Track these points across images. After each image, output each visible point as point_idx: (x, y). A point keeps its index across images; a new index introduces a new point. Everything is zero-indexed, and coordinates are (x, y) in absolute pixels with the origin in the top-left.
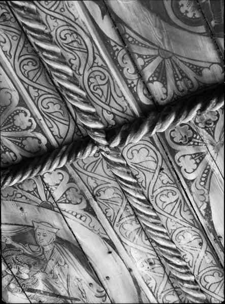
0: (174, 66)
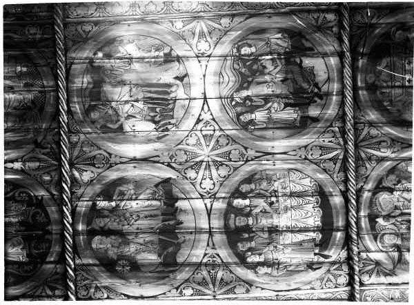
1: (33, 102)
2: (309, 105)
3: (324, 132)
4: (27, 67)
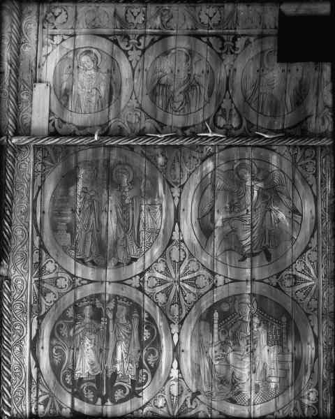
0: (53, 401)
1: (239, 392)
4: (276, 388)
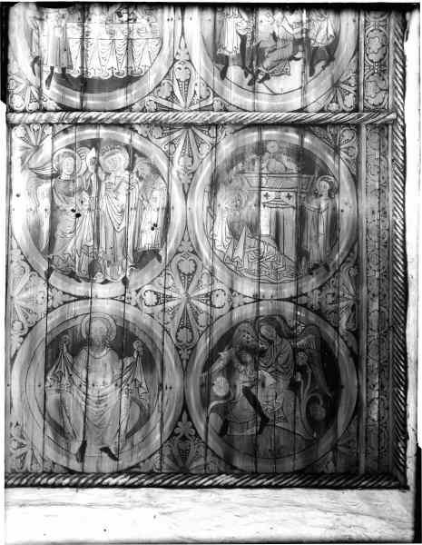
2: (243, 68)
3: (208, 86)
